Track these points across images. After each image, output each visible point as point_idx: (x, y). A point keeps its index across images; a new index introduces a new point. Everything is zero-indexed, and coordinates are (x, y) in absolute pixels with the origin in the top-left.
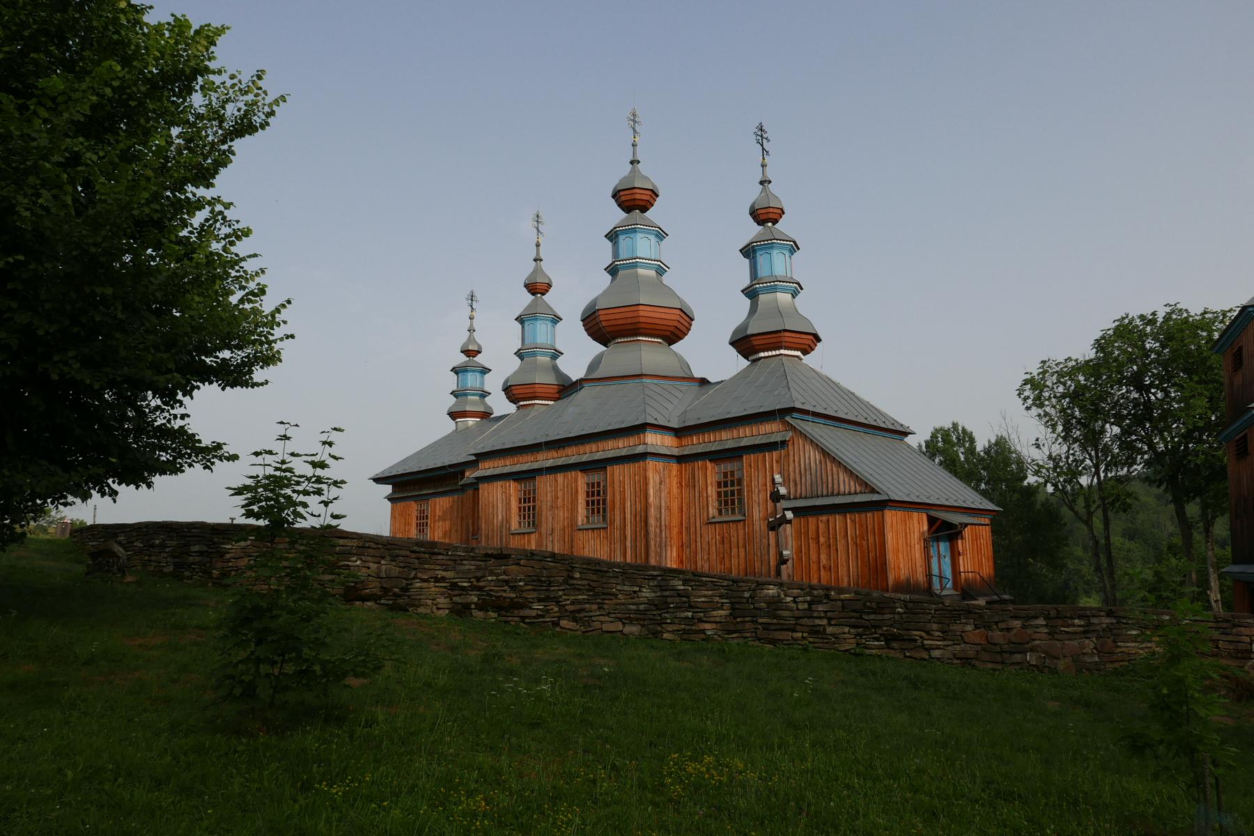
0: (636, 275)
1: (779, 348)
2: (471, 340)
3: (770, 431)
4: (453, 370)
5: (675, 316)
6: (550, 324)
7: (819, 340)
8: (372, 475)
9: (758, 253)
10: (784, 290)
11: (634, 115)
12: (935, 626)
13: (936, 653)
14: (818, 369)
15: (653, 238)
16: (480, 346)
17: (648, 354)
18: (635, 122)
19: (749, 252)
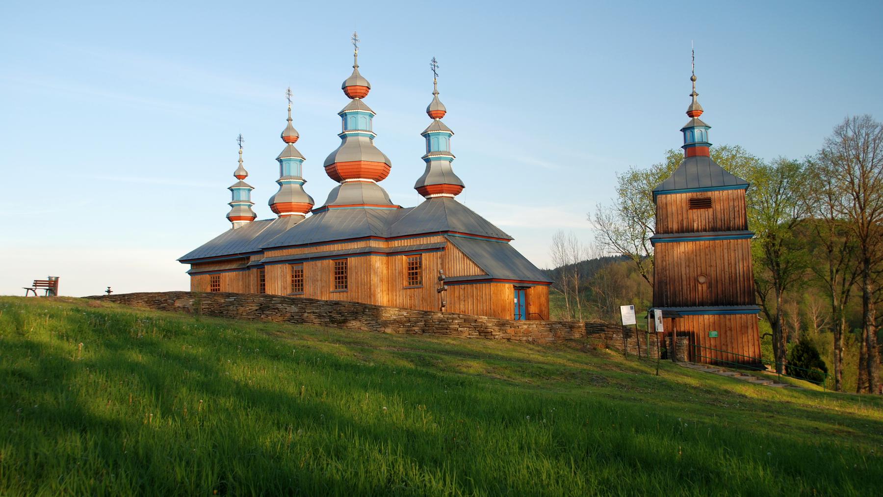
2: (240, 168)
3: (436, 240)
5: (381, 167)
8: (179, 257)
10: (446, 159)
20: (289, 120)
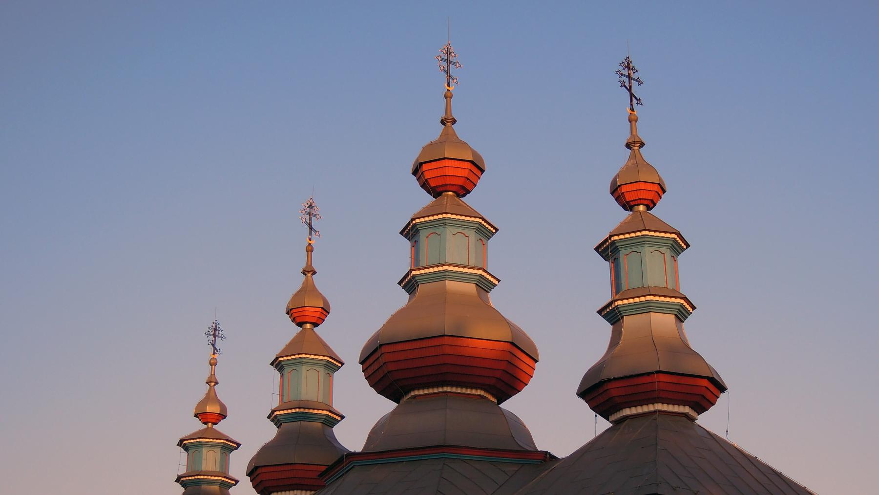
0: (444, 291)
1: (653, 401)
4: (181, 443)
6: (322, 370)
7: (722, 389)
9: (622, 253)
10: (663, 309)
11: (449, 53)
14: (722, 435)
15: (472, 235)
16: (223, 407)
17: (448, 416)
18: (449, 62)
19: (608, 250)
20: (308, 271)
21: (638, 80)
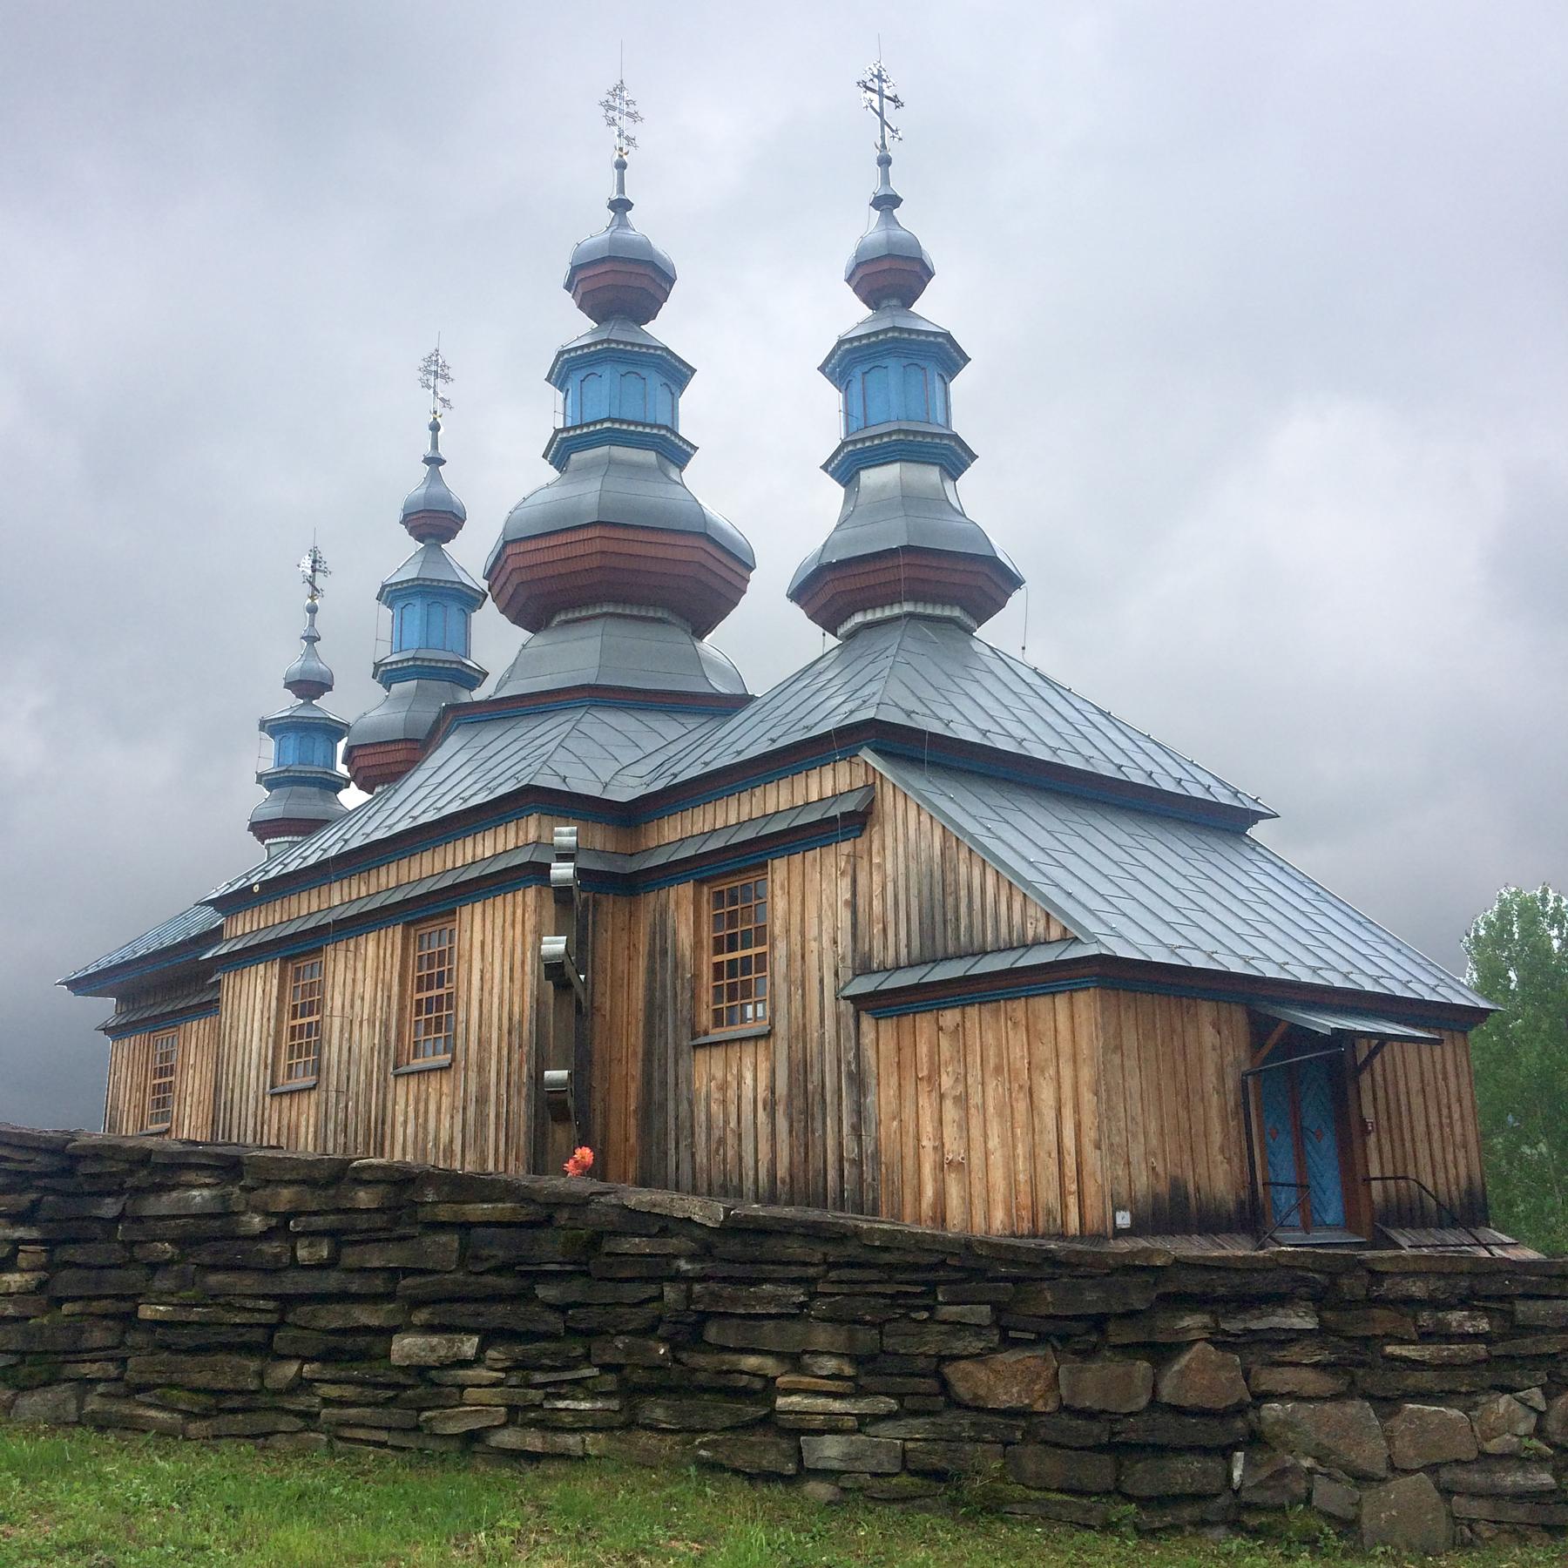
4: (263, 725)
12: (822, 1336)
13: (830, 1450)
21: (894, 100)
